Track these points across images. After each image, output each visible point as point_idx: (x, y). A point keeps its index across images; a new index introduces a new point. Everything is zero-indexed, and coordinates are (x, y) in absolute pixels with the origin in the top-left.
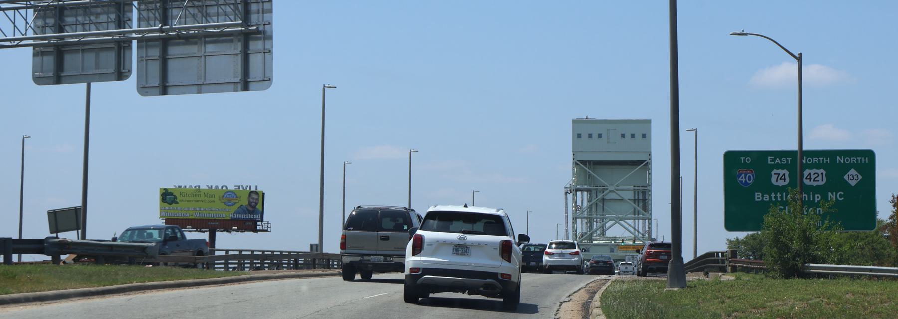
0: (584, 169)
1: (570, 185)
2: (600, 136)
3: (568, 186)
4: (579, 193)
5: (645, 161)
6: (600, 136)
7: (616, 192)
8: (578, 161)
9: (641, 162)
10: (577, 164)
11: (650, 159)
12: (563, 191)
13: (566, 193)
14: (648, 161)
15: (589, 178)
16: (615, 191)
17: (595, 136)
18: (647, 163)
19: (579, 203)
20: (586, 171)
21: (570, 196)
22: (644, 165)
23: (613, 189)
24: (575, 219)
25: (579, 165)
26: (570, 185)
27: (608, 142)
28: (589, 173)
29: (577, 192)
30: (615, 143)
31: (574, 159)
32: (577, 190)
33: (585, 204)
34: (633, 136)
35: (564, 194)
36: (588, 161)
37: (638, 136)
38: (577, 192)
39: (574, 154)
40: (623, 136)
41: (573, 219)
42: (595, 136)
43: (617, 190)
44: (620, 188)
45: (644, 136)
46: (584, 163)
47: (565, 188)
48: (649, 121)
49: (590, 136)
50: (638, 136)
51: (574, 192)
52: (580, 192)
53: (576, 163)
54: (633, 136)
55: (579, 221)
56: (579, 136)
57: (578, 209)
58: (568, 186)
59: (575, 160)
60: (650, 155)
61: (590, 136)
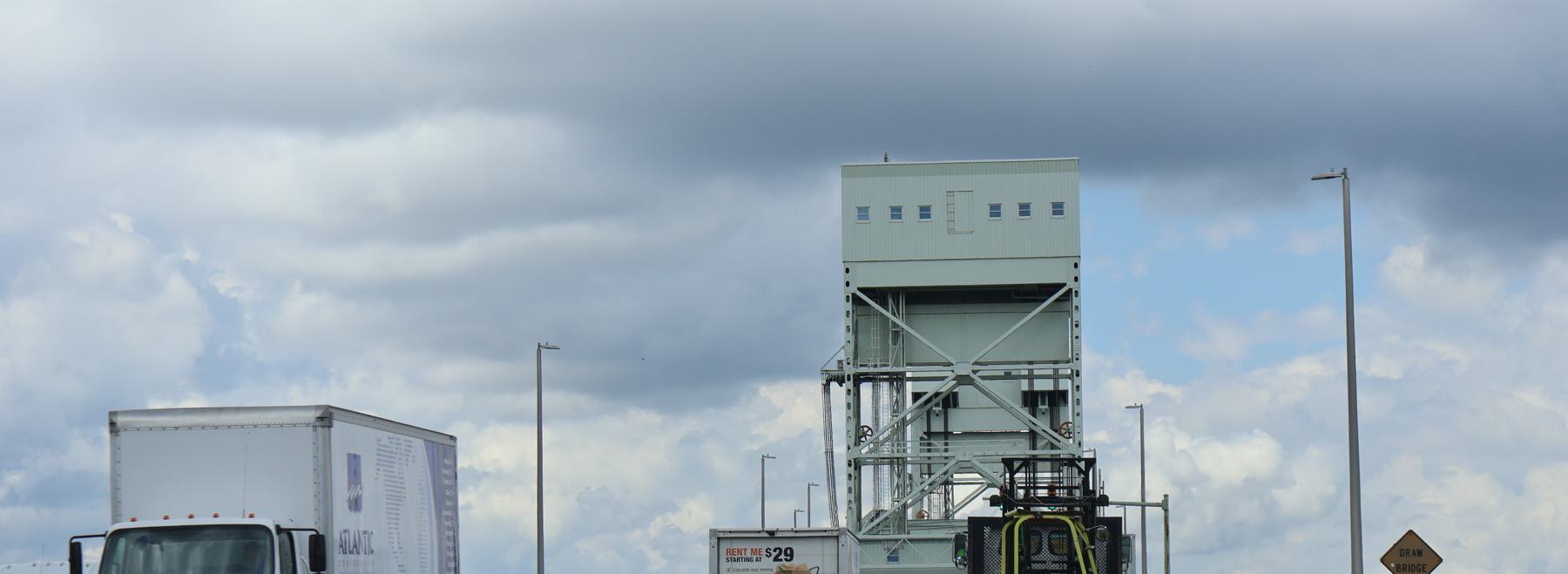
0: (882, 314)
1: (840, 362)
2: (925, 212)
5: (1064, 285)
6: (925, 212)
8: (859, 289)
10: (856, 300)
11: (1076, 279)
13: (826, 387)
14: (1071, 284)
17: (909, 213)
18: (1070, 290)
19: (866, 419)
24: (856, 464)
25: (868, 304)
26: (840, 362)
27: (951, 231)
28: (895, 325)
30: (972, 232)
32: (858, 379)
33: (886, 418)
35: (820, 388)
37: (1041, 209)
39: (847, 271)
40: (995, 210)
41: (850, 465)
42: (909, 213)
43: (983, 378)
45: (1058, 209)
46: (880, 294)
49: (896, 212)
50: (1041, 209)
51: (849, 384)
52: (871, 383)
53: (853, 294)
54: (1025, 210)
55: (867, 472)
56: (863, 212)
57: (865, 435)
58: (833, 366)
59: (853, 289)
60: (1076, 266)
61: (896, 212)
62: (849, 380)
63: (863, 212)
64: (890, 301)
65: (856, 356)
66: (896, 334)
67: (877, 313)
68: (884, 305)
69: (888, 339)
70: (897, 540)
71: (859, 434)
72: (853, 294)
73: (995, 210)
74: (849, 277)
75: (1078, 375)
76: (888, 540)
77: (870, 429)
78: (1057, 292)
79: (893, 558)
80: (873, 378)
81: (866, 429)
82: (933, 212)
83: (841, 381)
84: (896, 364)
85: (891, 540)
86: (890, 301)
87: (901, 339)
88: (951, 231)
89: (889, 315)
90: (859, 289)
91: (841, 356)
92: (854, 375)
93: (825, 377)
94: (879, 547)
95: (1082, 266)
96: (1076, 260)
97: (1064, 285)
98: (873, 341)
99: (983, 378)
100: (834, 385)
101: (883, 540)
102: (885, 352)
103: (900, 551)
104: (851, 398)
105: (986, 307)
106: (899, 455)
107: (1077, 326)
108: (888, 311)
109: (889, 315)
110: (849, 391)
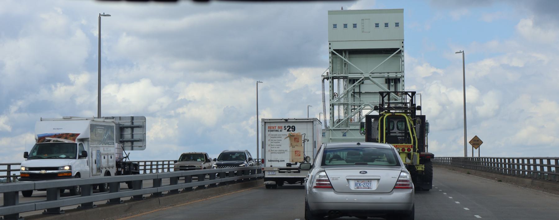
0: (341, 58)
1: (327, 73)
2: (355, 26)
3: (325, 74)
4: (336, 81)
5: (399, 49)
6: (355, 26)
7: (374, 79)
8: (334, 50)
10: (333, 53)
11: (403, 47)
12: (322, 78)
13: (323, 81)
14: (401, 48)
15: (345, 67)
16: (370, 77)
17: (350, 26)
18: (401, 50)
19: (336, 91)
20: (343, 59)
22: (397, 53)
23: (367, 76)
24: (332, 105)
25: (336, 54)
27: (363, 32)
28: (345, 61)
29: (334, 80)
30: (370, 32)
31: (330, 48)
32: (333, 78)
33: (342, 91)
34: (386, 25)
35: (321, 81)
36: (343, 50)
37: (392, 25)
38: (334, 80)
39: (330, 44)
40: (377, 25)
41: (331, 106)
42: (350, 26)
43: (373, 77)
44: (375, 75)
45: (397, 25)
46: (340, 51)
48: (401, 11)
49: (345, 26)
50: (392, 25)
52: (337, 79)
53: (332, 51)
54: (386, 25)
55: (336, 107)
56: (335, 26)
57: (335, 95)
58: (325, 74)
59: (332, 50)
60: (403, 43)
61: (345, 26)
62: (330, 78)
63: (335, 26)
64: (344, 54)
65: (332, 71)
66: (345, 64)
67: (339, 57)
68: (342, 55)
69: (343, 65)
70: (346, 130)
71: (333, 95)
72: (332, 51)
73: (377, 25)
74: (330, 46)
75: (403, 77)
76: (343, 129)
77: (337, 94)
78: (397, 51)
79: (344, 135)
80: (338, 78)
81: (335, 94)
82: (357, 26)
83: (328, 79)
84: (345, 73)
85: (344, 129)
86: (344, 54)
87: (347, 66)
88: (363, 32)
89: (343, 58)
90: (334, 50)
91: (328, 71)
92: (332, 77)
93: (323, 77)
94: (340, 132)
95: (404, 43)
96: (403, 41)
97: (399, 49)
98: (338, 66)
99: (373, 77)
100: (326, 80)
101: (342, 129)
102: (342, 69)
103: (346, 133)
104: (331, 84)
105: (374, 55)
106: (346, 102)
107: (403, 61)
108: (343, 56)
109: (343, 58)
110: (330, 82)
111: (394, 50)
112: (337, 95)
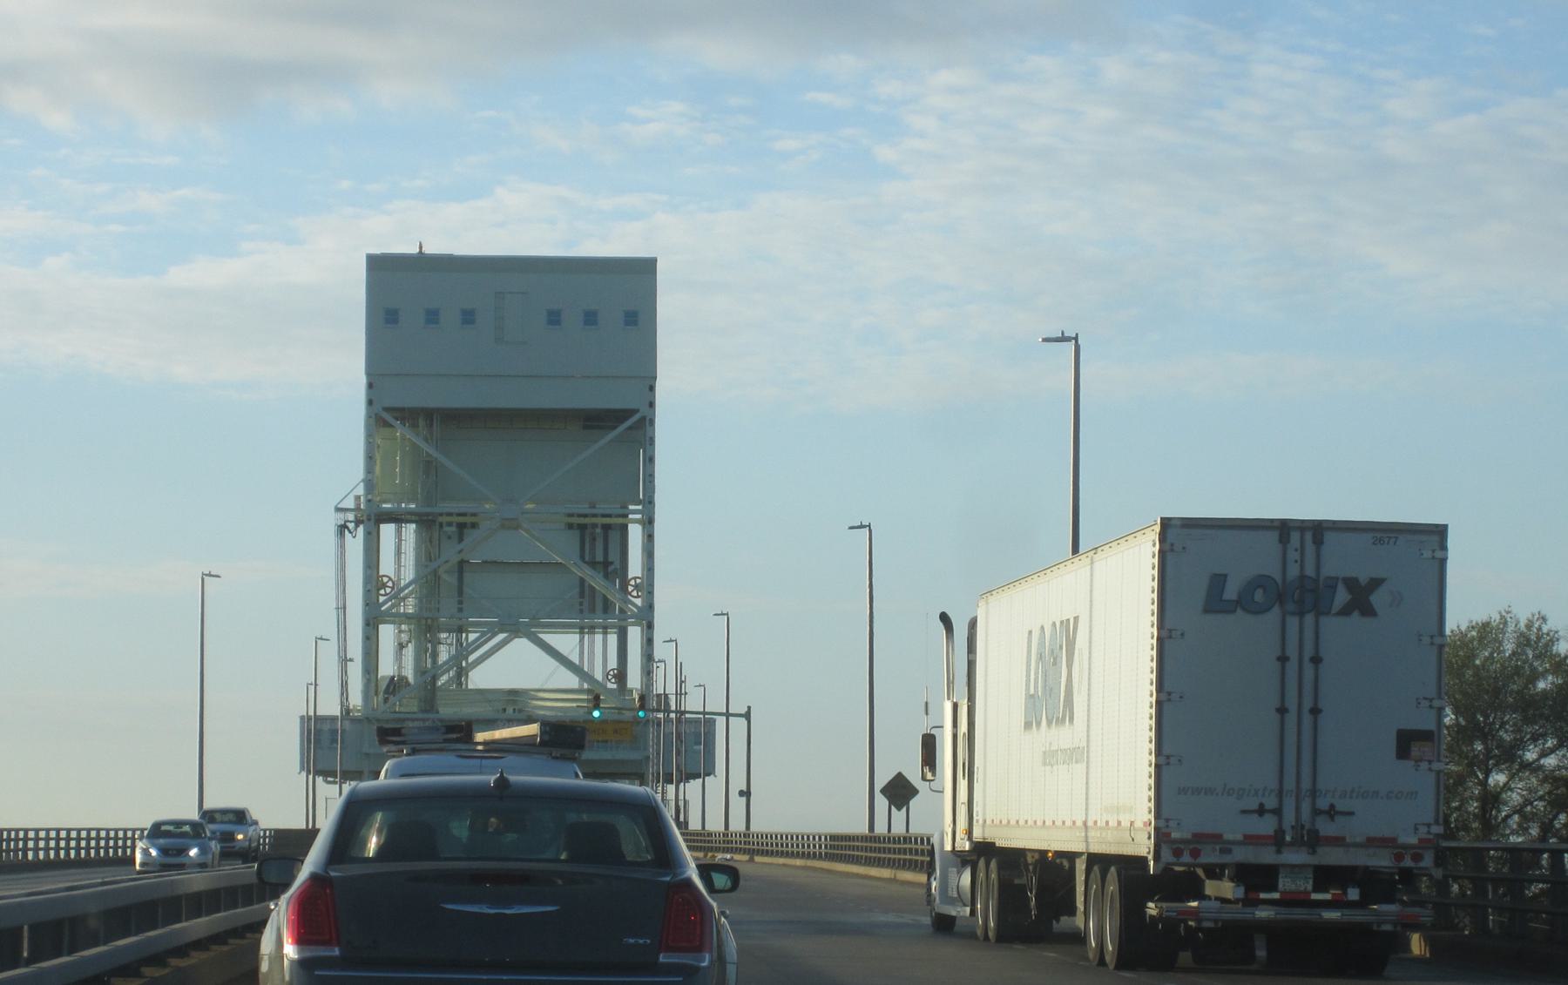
1: (357, 498)
2: (468, 317)
3: (350, 503)
4: (387, 531)
5: (637, 411)
8: (387, 409)
9: (624, 415)
12: (334, 520)
13: (342, 528)
14: (644, 410)
18: (643, 419)
19: (387, 567)
21: (355, 544)
22: (630, 428)
29: (382, 526)
34: (590, 318)
35: (332, 531)
38: (382, 526)
40: (554, 318)
46: (407, 415)
47: (338, 510)
55: (387, 633)
58: (350, 503)
61: (432, 317)
64: (421, 422)
77: (390, 579)
80: (396, 518)
81: (385, 580)
97: (637, 411)
111: (620, 416)
112: (390, 584)
